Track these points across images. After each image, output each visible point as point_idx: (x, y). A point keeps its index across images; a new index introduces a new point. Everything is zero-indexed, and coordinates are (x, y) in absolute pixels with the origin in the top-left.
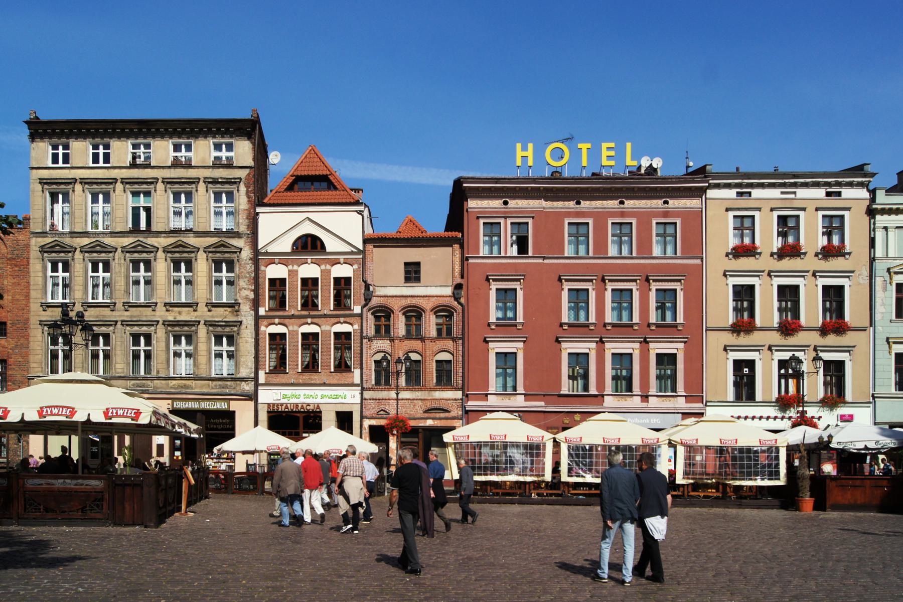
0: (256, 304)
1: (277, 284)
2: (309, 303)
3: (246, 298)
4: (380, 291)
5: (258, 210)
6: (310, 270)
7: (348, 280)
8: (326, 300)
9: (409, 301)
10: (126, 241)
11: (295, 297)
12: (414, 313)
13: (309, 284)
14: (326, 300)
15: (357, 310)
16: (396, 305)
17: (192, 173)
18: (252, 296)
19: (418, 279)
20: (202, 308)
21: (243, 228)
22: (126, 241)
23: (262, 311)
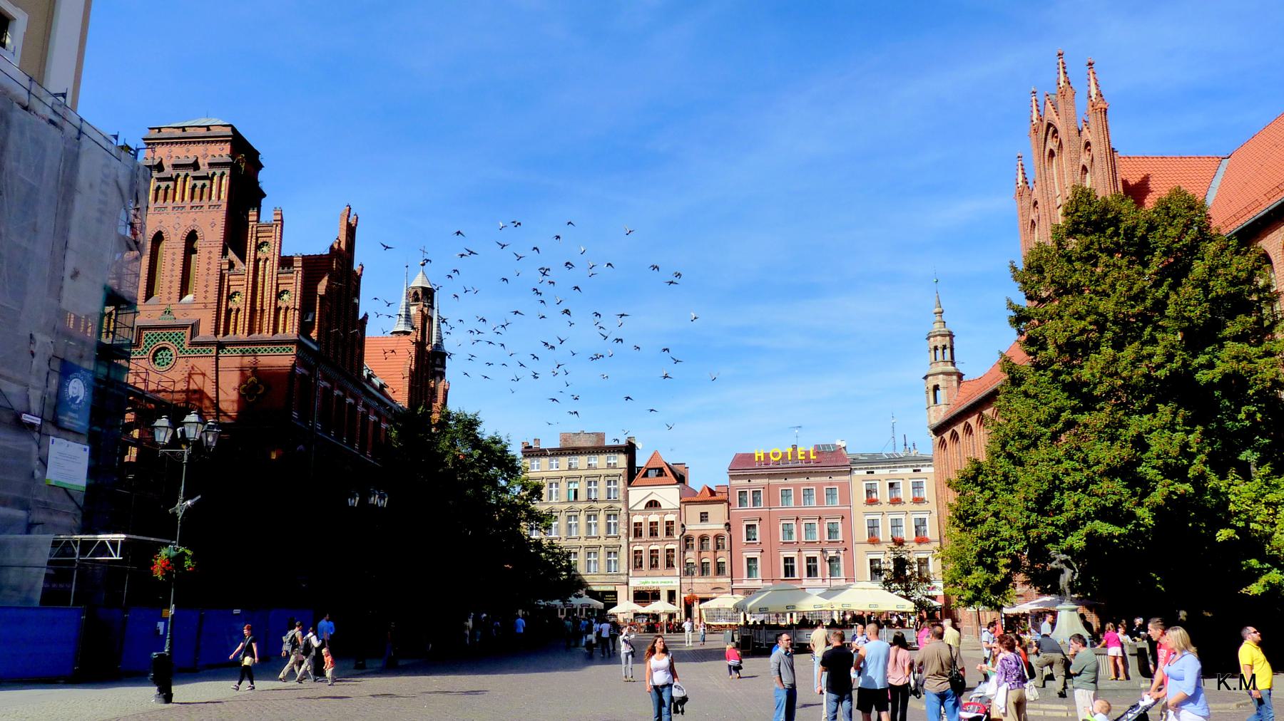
0: (628, 535)
1: (638, 525)
2: (653, 533)
3: (623, 533)
4: (687, 527)
5: (629, 489)
6: (654, 517)
7: (672, 522)
8: (661, 530)
9: (702, 533)
10: (566, 506)
11: (646, 530)
12: (703, 539)
13: (653, 524)
14: (661, 530)
15: (677, 537)
16: (696, 536)
17: (597, 472)
18: (626, 531)
19: (707, 520)
20: (603, 538)
21: (621, 498)
22: (566, 506)
23: (631, 539)
